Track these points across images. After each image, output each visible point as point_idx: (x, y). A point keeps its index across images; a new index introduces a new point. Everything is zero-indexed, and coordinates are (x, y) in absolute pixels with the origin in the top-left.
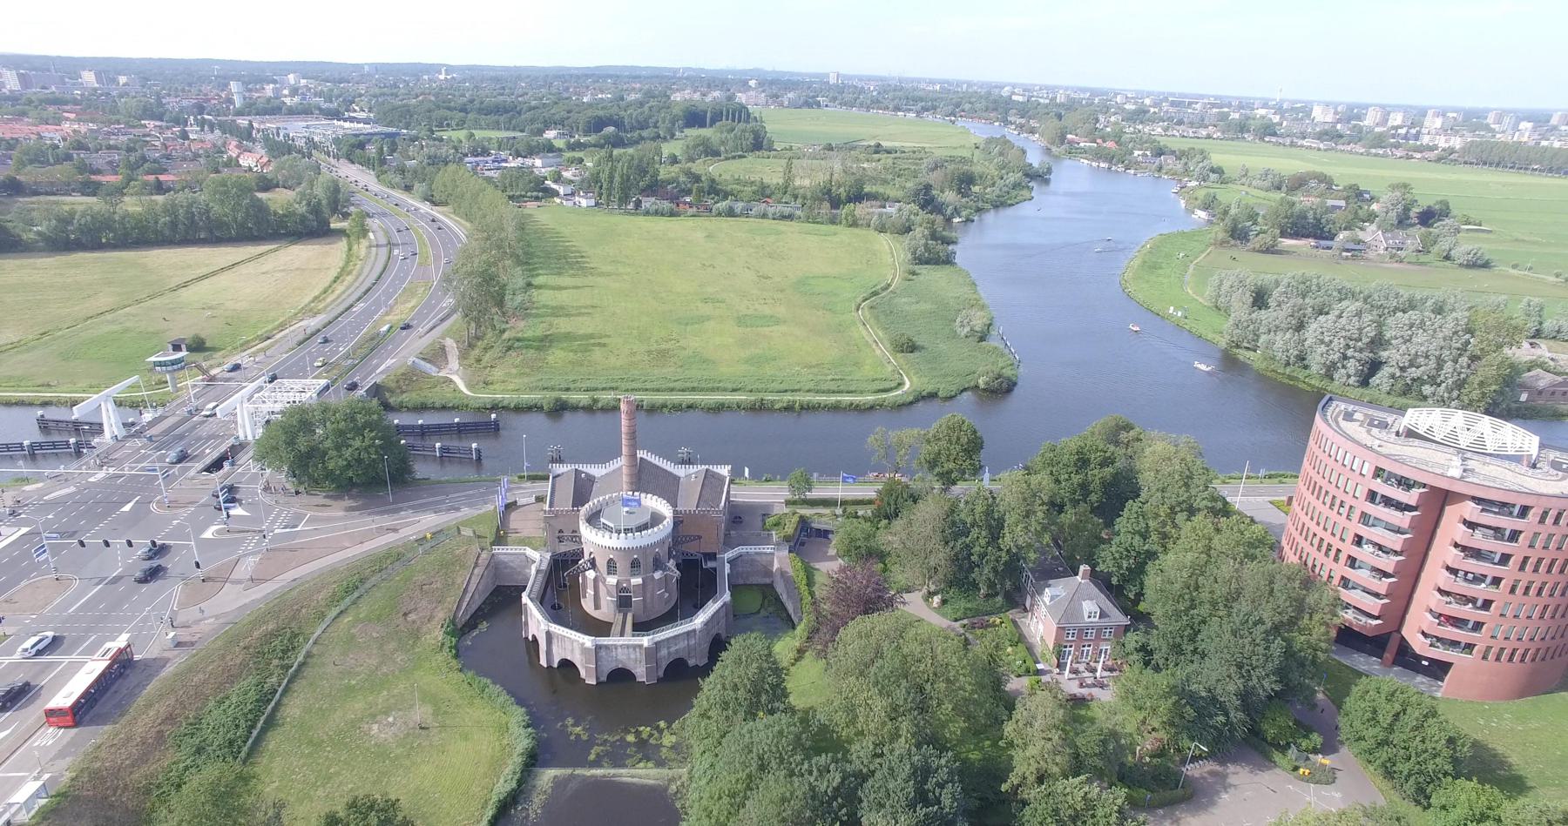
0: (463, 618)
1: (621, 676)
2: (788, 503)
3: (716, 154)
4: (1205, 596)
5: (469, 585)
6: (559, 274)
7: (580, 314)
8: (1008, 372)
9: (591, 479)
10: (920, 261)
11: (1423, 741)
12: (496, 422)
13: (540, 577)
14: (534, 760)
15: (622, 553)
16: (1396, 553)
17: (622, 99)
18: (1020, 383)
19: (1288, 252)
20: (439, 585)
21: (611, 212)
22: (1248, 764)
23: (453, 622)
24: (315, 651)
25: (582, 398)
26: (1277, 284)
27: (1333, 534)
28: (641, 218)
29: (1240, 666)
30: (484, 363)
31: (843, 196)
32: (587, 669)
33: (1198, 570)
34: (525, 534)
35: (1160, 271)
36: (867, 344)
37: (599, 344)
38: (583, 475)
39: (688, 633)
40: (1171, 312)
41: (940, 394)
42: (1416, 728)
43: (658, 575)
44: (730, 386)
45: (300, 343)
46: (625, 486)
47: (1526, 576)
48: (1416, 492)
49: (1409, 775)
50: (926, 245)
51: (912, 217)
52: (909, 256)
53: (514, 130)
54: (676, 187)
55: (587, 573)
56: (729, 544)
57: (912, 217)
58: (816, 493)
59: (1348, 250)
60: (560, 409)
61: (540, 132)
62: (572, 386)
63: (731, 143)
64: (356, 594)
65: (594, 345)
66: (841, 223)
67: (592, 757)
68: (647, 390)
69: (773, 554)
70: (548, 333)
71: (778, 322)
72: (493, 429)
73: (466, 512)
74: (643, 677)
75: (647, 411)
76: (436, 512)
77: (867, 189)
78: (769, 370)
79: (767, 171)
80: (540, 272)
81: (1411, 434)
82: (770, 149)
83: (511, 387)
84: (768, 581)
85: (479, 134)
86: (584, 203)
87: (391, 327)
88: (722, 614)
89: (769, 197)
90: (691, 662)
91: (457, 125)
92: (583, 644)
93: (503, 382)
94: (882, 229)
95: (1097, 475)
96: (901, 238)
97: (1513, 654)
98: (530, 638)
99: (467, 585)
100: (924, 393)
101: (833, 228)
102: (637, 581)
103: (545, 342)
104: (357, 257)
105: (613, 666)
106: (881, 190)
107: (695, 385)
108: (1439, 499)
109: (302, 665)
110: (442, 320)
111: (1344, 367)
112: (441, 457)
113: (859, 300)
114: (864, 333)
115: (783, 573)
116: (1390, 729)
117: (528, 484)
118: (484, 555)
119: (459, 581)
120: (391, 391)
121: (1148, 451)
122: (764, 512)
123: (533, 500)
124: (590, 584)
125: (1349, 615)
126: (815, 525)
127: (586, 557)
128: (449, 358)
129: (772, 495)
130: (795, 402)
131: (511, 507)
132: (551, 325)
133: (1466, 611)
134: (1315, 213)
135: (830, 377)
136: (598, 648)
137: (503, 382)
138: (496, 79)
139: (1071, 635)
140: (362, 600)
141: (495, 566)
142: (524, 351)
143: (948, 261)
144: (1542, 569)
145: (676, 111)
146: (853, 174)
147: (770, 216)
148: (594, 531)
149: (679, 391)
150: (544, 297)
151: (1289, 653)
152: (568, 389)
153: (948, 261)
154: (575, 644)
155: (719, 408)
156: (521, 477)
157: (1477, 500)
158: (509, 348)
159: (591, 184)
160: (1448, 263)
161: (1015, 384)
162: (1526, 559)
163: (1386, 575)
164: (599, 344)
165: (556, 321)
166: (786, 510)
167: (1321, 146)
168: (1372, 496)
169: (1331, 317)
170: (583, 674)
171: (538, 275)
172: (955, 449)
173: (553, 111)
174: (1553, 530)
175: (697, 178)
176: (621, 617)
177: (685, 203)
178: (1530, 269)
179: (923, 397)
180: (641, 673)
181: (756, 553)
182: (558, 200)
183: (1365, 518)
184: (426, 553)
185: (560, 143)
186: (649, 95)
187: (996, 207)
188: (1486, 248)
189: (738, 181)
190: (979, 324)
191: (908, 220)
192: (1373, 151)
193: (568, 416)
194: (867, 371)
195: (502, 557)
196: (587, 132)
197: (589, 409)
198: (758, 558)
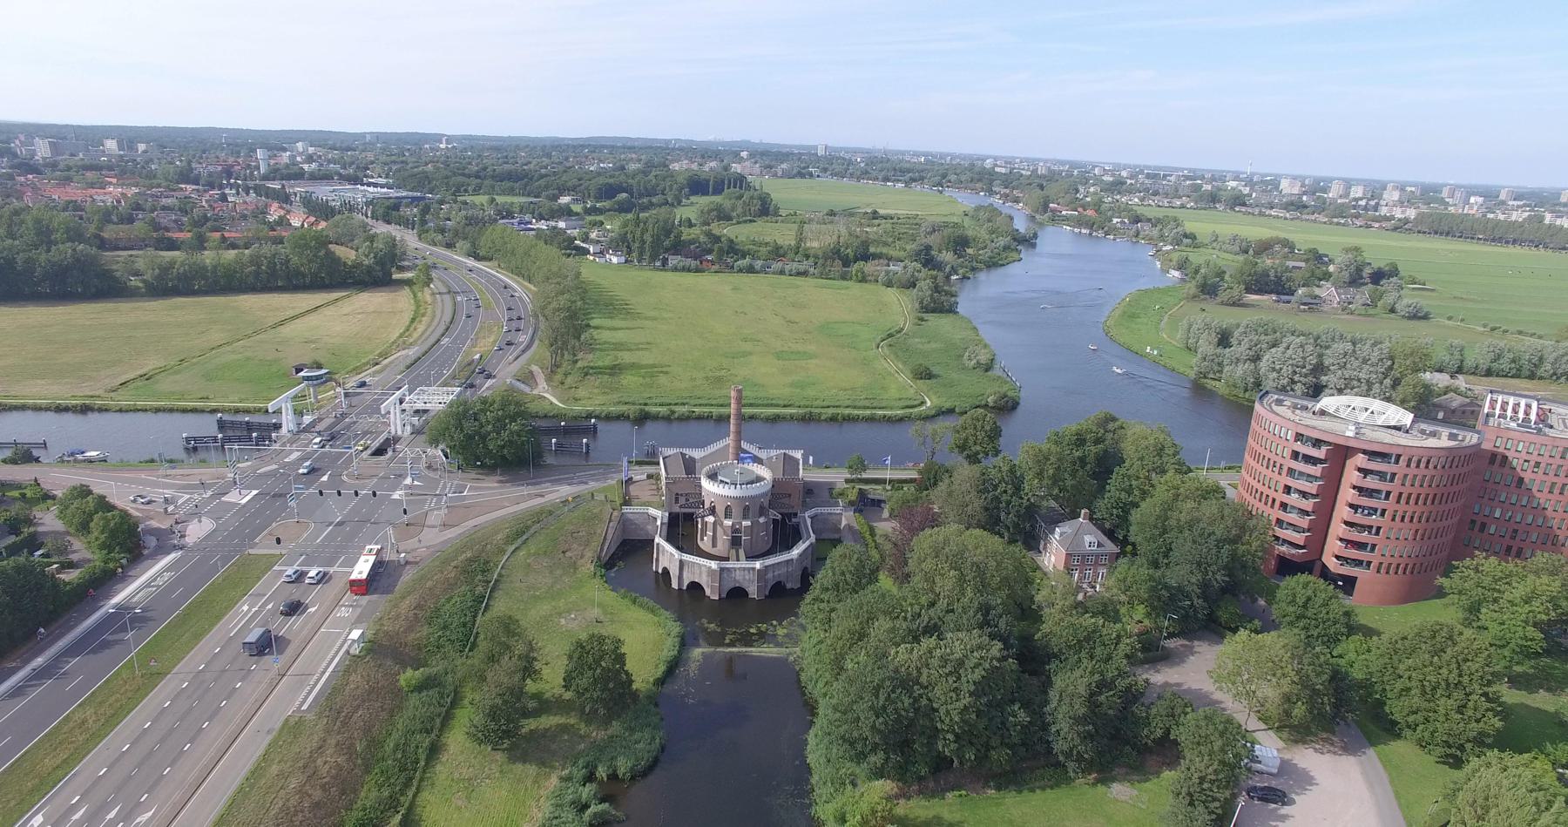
1: (738, 593)
2: (847, 481)
3: (729, 218)
4: (1173, 522)
5: (605, 535)
6: (611, 318)
7: (638, 349)
8: (1010, 394)
9: (693, 460)
10: (926, 309)
11: (1328, 613)
12: (594, 425)
13: (665, 527)
14: (685, 643)
16: (1314, 496)
17: (623, 168)
18: (1021, 402)
19: (1253, 306)
21: (641, 268)
22: (1209, 640)
24: (503, 572)
25: (663, 410)
26: (1238, 326)
27: (1270, 488)
28: (670, 274)
29: (1199, 564)
31: (851, 255)
33: (1168, 507)
35: (1139, 320)
36: (890, 374)
37: (662, 372)
39: (788, 561)
41: (957, 409)
42: (1323, 605)
43: (762, 520)
44: (781, 403)
45: (408, 367)
46: (730, 457)
47: (1402, 507)
48: (1324, 449)
49: (1318, 637)
50: (932, 295)
51: (916, 274)
52: (917, 305)
53: (529, 195)
54: (697, 247)
55: (706, 519)
56: (806, 506)
57: (916, 274)
59: (1305, 304)
60: (643, 418)
61: (555, 198)
62: (648, 401)
63: (739, 210)
64: (525, 537)
66: (851, 279)
67: (727, 641)
73: (592, 485)
77: (872, 250)
78: (811, 392)
79: (783, 235)
81: (1323, 413)
82: (776, 214)
83: (597, 402)
85: (500, 199)
86: (615, 260)
87: (481, 356)
88: (810, 552)
89: (783, 256)
90: (789, 586)
91: (474, 190)
94: (889, 284)
95: (1092, 450)
96: (908, 292)
97: (1398, 568)
98: (660, 571)
100: (943, 409)
101: (845, 283)
102: (746, 523)
103: (615, 370)
104: (426, 303)
105: (732, 585)
106: (885, 250)
108: (1341, 453)
109: (496, 581)
110: (524, 351)
111: (1292, 390)
112: (556, 450)
113: (878, 340)
114: (886, 365)
115: (849, 527)
116: (1305, 606)
117: (637, 467)
119: (599, 531)
121: (1129, 433)
122: (830, 487)
123: (645, 477)
124: (710, 527)
125: (1284, 549)
127: (707, 505)
129: (837, 476)
132: (617, 358)
133: (1364, 537)
134: (1276, 272)
135: (864, 397)
136: (722, 570)
138: (497, 149)
139: (1076, 560)
141: (624, 522)
142: (600, 376)
143: (951, 310)
144: (1412, 501)
145: (681, 179)
146: (857, 237)
148: (716, 485)
150: (605, 336)
151: (1234, 556)
153: (951, 310)
155: (776, 419)
157: (1365, 452)
158: (586, 374)
159: (622, 244)
160: (1392, 315)
161: (1018, 404)
162: (1401, 494)
163: (1307, 513)
164: (662, 372)
165: (620, 354)
167: (1288, 215)
168: (1295, 455)
169: (1281, 349)
170: (708, 592)
171: (593, 318)
172: (981, 435)
173: (564, 178)
174: (1426, 472)
175: (717, 239)
176: (734, 551)
177: (708, 261)
178: (1462, 320)
179: (943, 412)
180: (753, 591)
183: (1291, 472)
185: (577, 208)
186: (649, 166)
187: (989, 267)
188: (1425, 302)
189: (754, 243)
190: (984, 358)
191: (913, 276)
192: (1335, 220)
193: (650, 427)
194: (893, 392)
195: (630, 516)
196: (599, 198)
197: (668, 419)
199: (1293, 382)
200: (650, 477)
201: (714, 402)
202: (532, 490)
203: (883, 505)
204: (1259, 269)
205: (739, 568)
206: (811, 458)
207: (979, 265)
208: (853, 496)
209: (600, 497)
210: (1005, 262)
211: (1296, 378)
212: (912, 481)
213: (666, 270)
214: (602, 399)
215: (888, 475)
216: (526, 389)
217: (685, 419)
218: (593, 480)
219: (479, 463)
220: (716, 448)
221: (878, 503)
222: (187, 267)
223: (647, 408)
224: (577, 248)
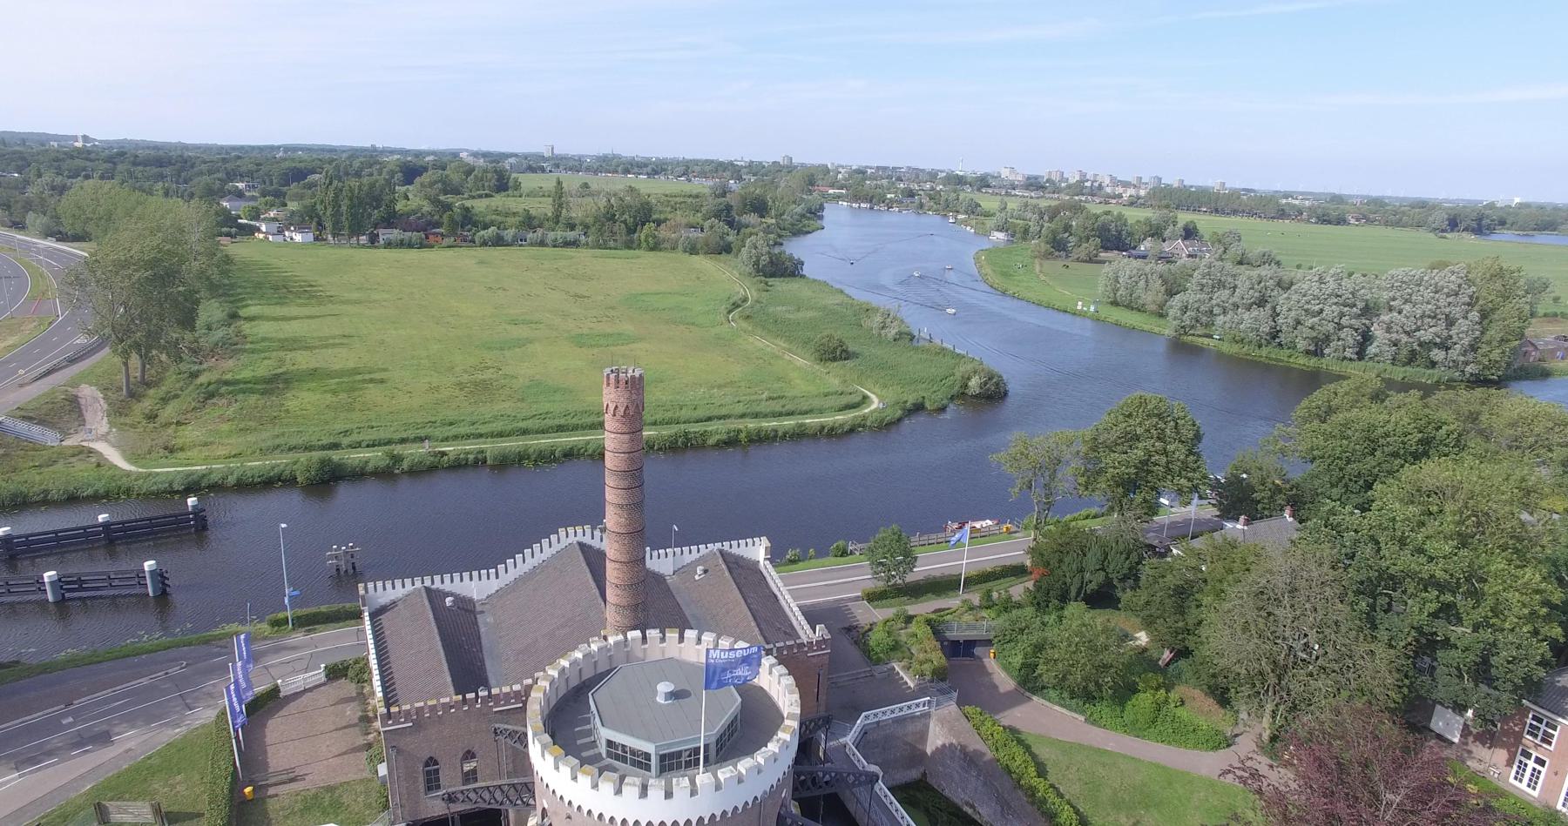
2: (873, 597)
6: (282, 304)
7: (326, 347)
9: (466, 607)
12: (198, 511)
25: (375, 457)
30: (162, 419)
37: (371, 381)
38: (449, 601)
40: (1079, 307)
41: (928, 405)
46: (611, 614)
58: (929, 564)
65: (364, 381)
66: (639, 247)
68: (481, 436)
69: (927, 715)
70: (280, 371)
71: (641, 339)
72: (198, 526)
75: (493, 467)
80: (250, 302)
83: (222, 451)
84: (914, 774)
86: (298, 237)
93: (206, 444)
103: (276, 384)
107: (562, 422)
110: (72, 361)
115: (969, 759)
117: (299, 637)
123: (319, 675)
128: (88, 416)
130: (739, 431)
131: (264, 705)
132: (282, 361)
137: (206, 444)
142: (240, 397)
147: (548, 241)
149: (537, 432)
150: (264, 329)
156: (278, 623)
158: (211, 395)
164: (371, 381)
165: (290, 355)
171: (247, 306)
175: (448, 207)
181: (897, 721)
182: (261, 236)
193: (345, 494)
197: (385, 474)
199: (1340, 327)
200: (336, 673)
201: (483, 429)
203: (978, 651)
207: (783, 233)
210: (807, 229)
211: (1344, 321)
213: (376, 247)
214: (237, 443)
216: (50, 438)
217: (420, 471)
218: (131, 720)
220: (531, 562)
223: (335, 456)
224: (242, 227)
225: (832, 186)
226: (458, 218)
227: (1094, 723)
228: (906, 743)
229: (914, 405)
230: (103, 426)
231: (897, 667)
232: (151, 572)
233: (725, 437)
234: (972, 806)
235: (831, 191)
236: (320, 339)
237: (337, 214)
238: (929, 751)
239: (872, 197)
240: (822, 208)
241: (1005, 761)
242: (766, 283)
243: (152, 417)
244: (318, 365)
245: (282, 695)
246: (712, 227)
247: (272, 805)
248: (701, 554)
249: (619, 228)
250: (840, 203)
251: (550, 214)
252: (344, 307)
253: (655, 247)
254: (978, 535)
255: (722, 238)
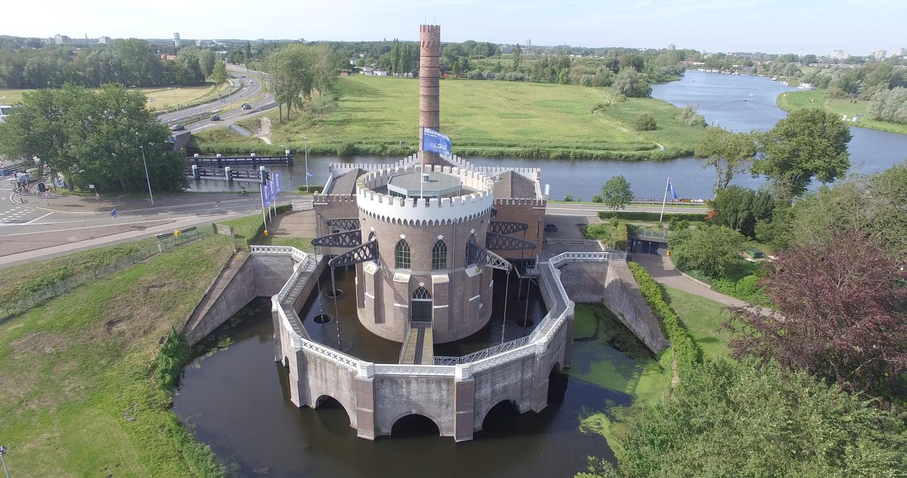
0: (196, 332)
2: (602, 215)
13: (304, 280)
15: (420, 231)
20: (172, 288)
23: (181, 337)
32: (359, 414)
34: (295, 234)
37: (388, 123)
41: (696, 153)
43: (472, 271)
56: (548, 251)
73: (232, 215)
74: (451, 430)
76: (198, 214)
84: (596, 298)
86: (379, 73)
88: (563, 334)
90: (524, 407)
92: (353, 374)
99: (211, 291)
100: (682, 152)
102: (440, 277)
105: (401, 411)
110: (263, 109)
115: (622, 286)
118: (241, 256)
119: (201, 285)
120: (203, 140)
124: (369, 284)
126: (643, 237)
127: (365, 239)
128: (263, 128)
135: (592, 140)
140: (54, 303)
147: (507, 78)
150: (347, 104)
152: (360, 143)
154: (342, 373)
156: (302, 189)
164: (388, 123)
165: (355, 113)
166: (601, 222)
170: (354, 421)
176: (415, 332)
181: (586, 262)
184: (168, 250)
198: (588, 268)
202: (139, 220)
203: (660, 251)
204: (893, 73)
205: (418, 378)
206: (547, 187)
208: (620, 233)
209: (224, 231)
210: (670, 80)
212: (701, 218)
215: (663, 210)
216: (245, 133)
219: (92, 186)
221: (651, 248)
222: (36, 65)
225: (696, 61)
226: (461, 66)
227: (716, 290)
228: (592, 278)
229: (687, 152)
230: (267, 132)
231: (599, 242)
232: (263, 171)
233: (560, 154)
234: (622, 316)
235: (695, 63)
236: (371, 109)
237: (397, 61)
238: (605, 287)
239: (721, 66)
240: (683, 70)
241: (644, 289)
242: (625, 98)
243: (287, 131)
244: (366, 117)
245: (293, 210)
246: (601, 71)
247: (273, 240)
248: (502, 172)
249: (548, 70)
250: (699, 70)
251: (512, 65)
252: (389, 98)
253: (568, 82)
254: (689, 203)
255: (607, 77)
